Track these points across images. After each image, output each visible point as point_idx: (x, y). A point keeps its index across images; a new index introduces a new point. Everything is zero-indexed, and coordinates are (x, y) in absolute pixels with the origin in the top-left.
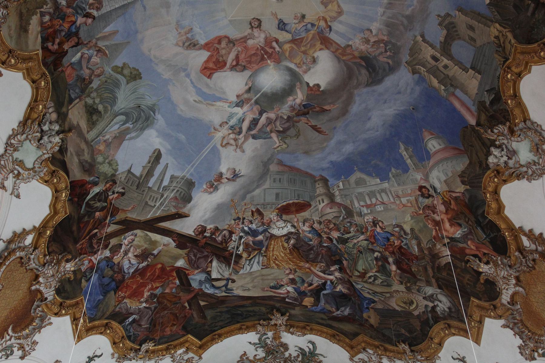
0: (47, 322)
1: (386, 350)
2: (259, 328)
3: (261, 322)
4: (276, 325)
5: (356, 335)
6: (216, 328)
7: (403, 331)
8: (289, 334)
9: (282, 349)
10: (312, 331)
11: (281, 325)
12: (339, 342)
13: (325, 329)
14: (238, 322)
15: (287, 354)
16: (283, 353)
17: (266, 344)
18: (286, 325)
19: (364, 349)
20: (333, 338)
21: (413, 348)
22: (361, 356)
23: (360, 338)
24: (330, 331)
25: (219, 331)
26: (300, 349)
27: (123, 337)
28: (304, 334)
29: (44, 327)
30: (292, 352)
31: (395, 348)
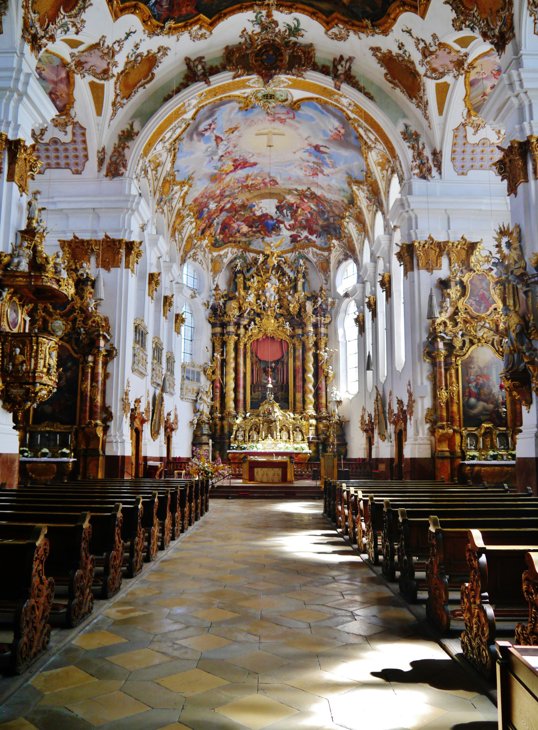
0: (88, 3)
1: (353, 25)
2: (256, 8)
3: (257, 2)
4: (268, 5)
5: (331, 12)
6: (222, 8)
7: (368, 9)
8: (279, 13)
9: (273, 25)
10: (297, 9)
11: (272, 5)
12: (317, 19)
13: (307, 8)
14: (239, 3)
15: (277, 30)
16: (274, 28)
17: (262, 21)
18: (277, 5)
19: (337, 25)
20: (312, 15)
21: (374, 23)
22: (335, 30)
23: (334, 15)
24: (311, 10)
25: (224, 11)
26: (288, 25)
27: (150, 16)
28: (291, 13)
29: (87, 7)
30: (282, 27)
31: (360, 24)
